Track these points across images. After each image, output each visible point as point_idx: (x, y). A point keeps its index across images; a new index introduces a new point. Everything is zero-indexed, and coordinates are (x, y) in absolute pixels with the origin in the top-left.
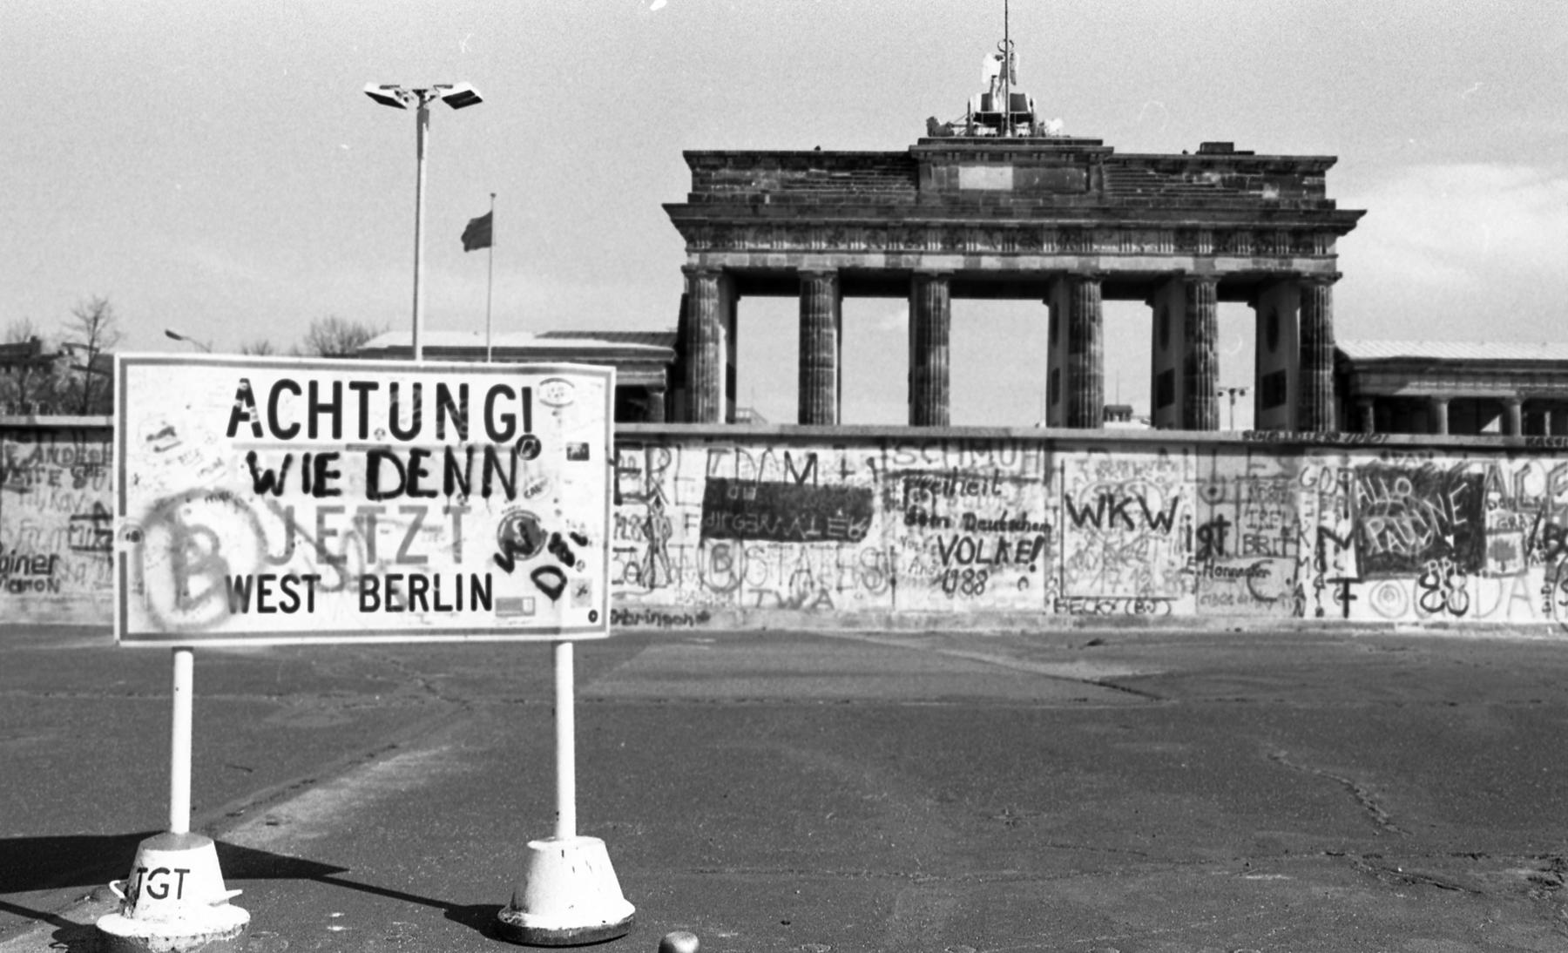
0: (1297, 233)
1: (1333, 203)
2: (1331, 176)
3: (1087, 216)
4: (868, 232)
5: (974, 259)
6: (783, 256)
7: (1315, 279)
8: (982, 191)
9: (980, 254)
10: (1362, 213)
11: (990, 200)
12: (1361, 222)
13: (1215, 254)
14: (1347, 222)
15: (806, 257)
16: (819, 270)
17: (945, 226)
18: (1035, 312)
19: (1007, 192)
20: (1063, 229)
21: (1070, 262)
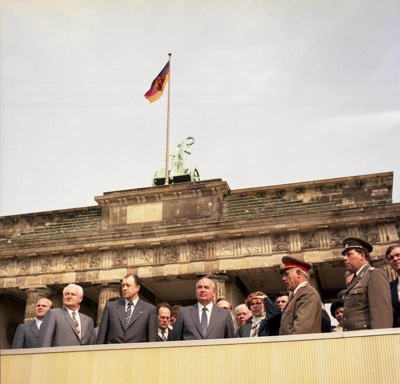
3: (206, 230)
4: (66, 259)
5: (132, 270)
6: (14, 279)
8: (140, 224)
11: (147, 229)
13: (303, 250)
15: (28, 277)
16: (32, 287)
17: (113, 250)
19: (157, 223)
20: (194, 243)
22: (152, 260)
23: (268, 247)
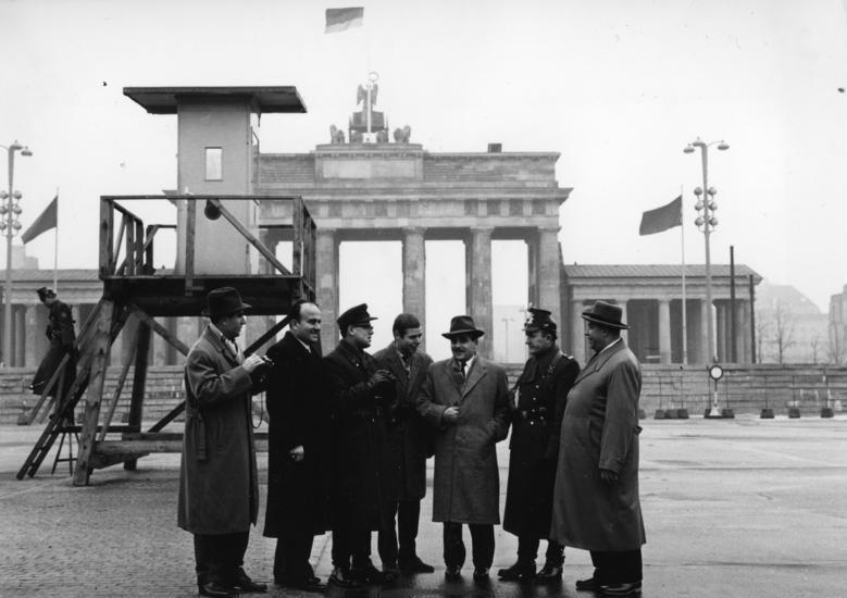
0: (535, 202)
1: (556, 184)
2: (558, 166)
7: (546, 230)
9: (351, 218)
10: (570, 190)
12: (571, 195)
14: (561, 196)
17: (330, 203)
18: (396, 246)
20: (399, 202)
21: (403, 223)
22: (365, 213)
23: (461, 209)
